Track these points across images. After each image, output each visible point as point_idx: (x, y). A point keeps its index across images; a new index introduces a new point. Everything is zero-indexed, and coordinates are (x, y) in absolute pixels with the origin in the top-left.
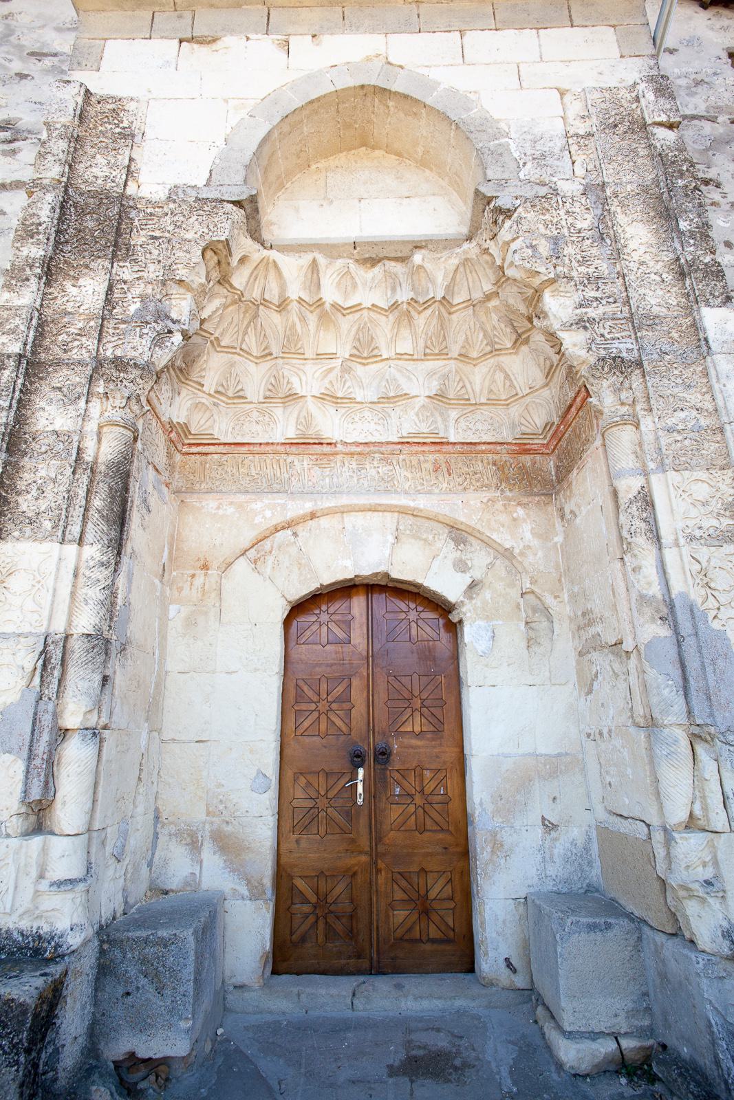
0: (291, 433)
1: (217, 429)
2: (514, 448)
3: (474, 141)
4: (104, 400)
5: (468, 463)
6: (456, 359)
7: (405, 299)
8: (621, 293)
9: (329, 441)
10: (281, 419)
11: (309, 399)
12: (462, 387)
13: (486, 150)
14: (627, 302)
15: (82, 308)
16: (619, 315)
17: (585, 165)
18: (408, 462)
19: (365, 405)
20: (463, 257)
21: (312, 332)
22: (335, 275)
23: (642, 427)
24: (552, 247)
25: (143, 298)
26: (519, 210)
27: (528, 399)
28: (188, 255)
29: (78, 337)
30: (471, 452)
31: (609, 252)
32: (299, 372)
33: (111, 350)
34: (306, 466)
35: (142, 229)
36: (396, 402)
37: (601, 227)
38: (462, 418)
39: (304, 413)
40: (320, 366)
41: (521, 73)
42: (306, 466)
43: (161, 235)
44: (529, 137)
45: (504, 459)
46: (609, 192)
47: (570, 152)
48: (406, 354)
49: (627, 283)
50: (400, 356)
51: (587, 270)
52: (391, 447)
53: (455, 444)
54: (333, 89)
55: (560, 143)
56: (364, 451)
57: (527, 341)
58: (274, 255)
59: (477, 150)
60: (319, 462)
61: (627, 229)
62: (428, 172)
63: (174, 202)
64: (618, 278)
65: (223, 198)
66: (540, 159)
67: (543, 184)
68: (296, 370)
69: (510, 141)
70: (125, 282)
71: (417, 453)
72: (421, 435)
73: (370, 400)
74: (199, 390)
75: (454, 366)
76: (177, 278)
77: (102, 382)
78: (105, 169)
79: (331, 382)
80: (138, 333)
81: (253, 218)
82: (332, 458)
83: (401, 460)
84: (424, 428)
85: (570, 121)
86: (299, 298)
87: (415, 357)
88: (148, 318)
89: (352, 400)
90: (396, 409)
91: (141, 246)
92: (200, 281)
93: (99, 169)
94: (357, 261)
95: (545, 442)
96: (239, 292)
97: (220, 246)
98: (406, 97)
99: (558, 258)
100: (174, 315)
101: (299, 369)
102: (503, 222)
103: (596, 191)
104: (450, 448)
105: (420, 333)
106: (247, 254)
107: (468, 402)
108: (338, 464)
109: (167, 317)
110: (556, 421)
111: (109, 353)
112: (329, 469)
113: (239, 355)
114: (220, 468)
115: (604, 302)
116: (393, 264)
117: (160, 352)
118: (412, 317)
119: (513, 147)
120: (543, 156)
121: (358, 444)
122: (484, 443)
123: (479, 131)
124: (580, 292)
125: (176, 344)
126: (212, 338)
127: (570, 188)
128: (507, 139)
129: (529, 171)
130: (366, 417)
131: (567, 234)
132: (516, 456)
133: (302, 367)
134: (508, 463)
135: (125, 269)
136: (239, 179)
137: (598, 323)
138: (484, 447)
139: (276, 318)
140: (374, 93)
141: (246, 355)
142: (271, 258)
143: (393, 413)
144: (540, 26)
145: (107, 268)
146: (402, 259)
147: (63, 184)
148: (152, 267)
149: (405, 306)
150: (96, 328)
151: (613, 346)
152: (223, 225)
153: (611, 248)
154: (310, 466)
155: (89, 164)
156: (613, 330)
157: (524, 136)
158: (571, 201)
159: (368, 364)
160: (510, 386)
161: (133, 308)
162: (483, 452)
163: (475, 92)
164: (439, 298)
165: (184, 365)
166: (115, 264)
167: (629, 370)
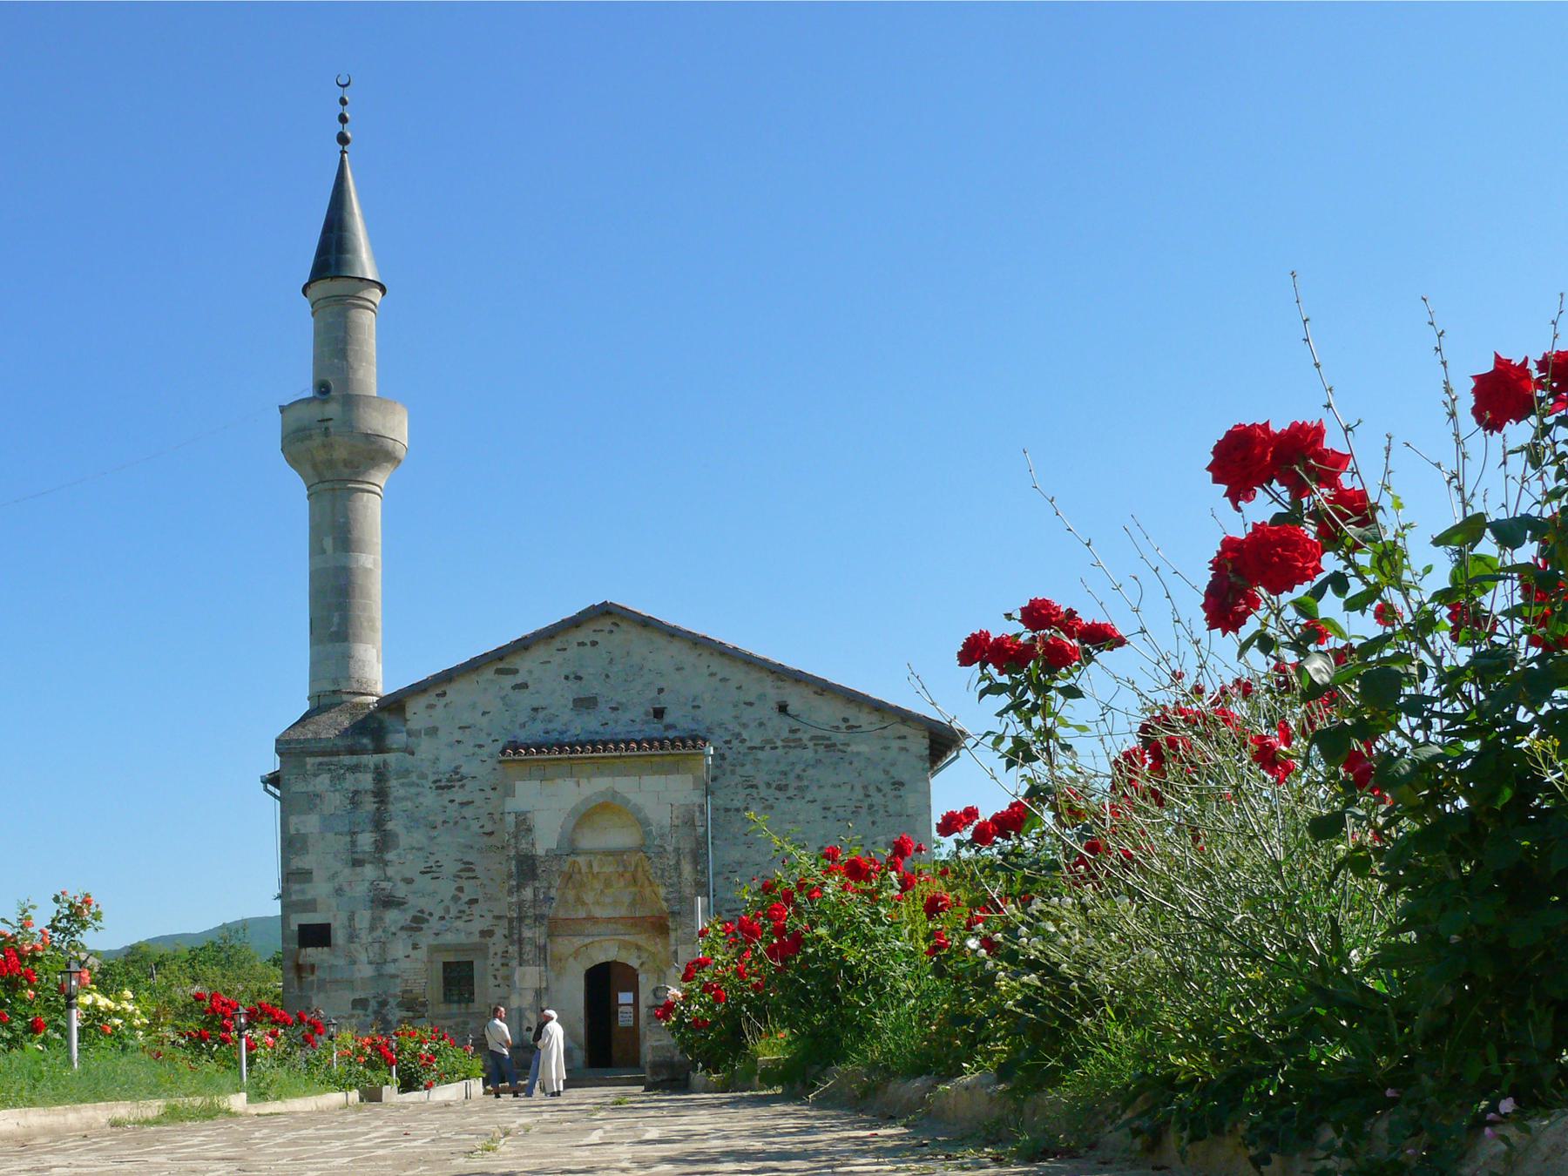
0: (584, 916)
56: (609, 920)
66: (662, 836)
103: (677, 850)
127: (670, 849)
144: (668, 772)
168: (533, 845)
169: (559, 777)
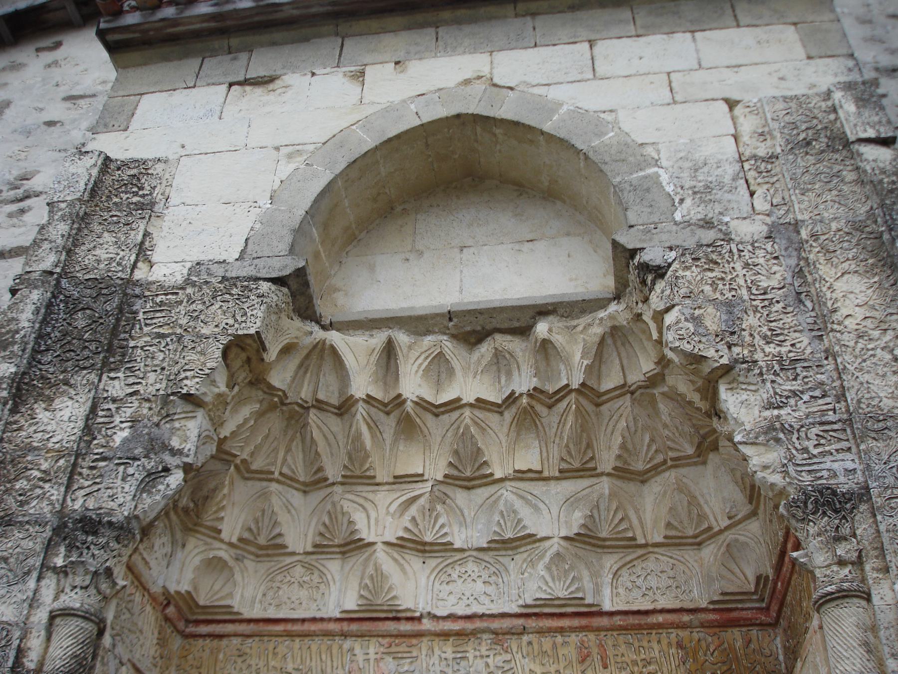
0: (351, 603)
1: (238, 597)
2: (712, 616)
3: (609, 174)
4: (62, 575)
5: (636, 644)
6: (609, 475)
7: (524, 389)
8: (833, 381)
9: (409, 614)
10: (337, 578)
11: (380, 547)
12: (622, 520)
13: (627, 186)
14: (841, 396)
15: (54, 440)
16: (831, 417)
17: (769, 198)
18: (536, 646)
19: (467, 554)
20: (609, 324)
21: (388, 442)
22: (420, 361)
23: (875, 599)
24: (724, 317)
25: (134, 421)
26: (675, 266)
27: (729, 536)
28: (202, 359)
29: (41, 483)
30: (640, 627)
31: (810, 320)
32: (368, 505)
33: (80, 502)
34: (372, 656)
35: (146, 325)
36: (516, 548)
37: (796, 284)
38: (625, 569)
39: (370, 570)
40: (399, 494)
41: (673, 85)
42: (372, 656)
43: (170, 331)
44: (687, 164)
45: (696, 636)
46: (804, 234)
47: (747, 181)
48: (530, 471)
49: (841, 367)
50: (521, 476)
51: (778, 349)
52: (506, 623)
53: (611, 614)
54: (417, 122)
55: (731, 169)
57: (715, 448)
58: (334, 337)
59: (614, 187)
60: (393, 649)
61: (837, 285)
62: (559, 203)
63: (193, 284)
64: (826, 358)
65: (259, 275)
66: (704, 193)
67: (707, 224)
68: (361, 501)
69: (661, 171)
70: (114, 400)
71: (550, 630)
72: (556, 602)
73: (476, 545)
74: (215, 538)
75: (606, 486)
76: (184, 391)
77: (62, 549)
78: (111, 249)
79: (413, 519)
80: (121, 474)
81: (302, 294)
82: (414, 641)
83: (524, 644)
84: (560, 591)
85: (745, 139)
86: (368, 395)
87: (546, 474)
88: (136, 452)
89: (447, 548)
90: (516, 557)
91: (142, 348)
92: (216, 390)
93: (104, 251)
94: (454, 337)
95: (764, 605)
96: (280, 393)
97: (249, 341)
98: (517, 124)
99: (733, 333)
100: (175, 443)
101: (366, 498)
102: (654, 283)
104: (605, 621)
105: (553, 435)
106: (295, 341)
107: (633, 543)
108: (424, 653)
109: (166, 447)
110: (770, 573)
111: (77, 505)
112: (409, 660)
113: (278, 481)
114: (240, 660)
115: (806, 397)
116: (509, 337)
117: (149, 501)
118: (537, 414)
119: (664, 177)
120: (708, 189)
121: (452, 617)
122: (662, 611)
123: (616, 161)
124: (768, 385)
125: (173, 486)
126: (238, 461)
128: (656, 169)
129: (688, 210)
130: (470, 572)
131: (746, 297)
132: (717, 630)
133: (370, 496)
134: (703, 644)
135: (116, 382)
136: (283, 247)
137: (798, 431)
138: (660, 618)
139: (334, 423)
140: (474, 121)
141: (289, 482)
142: (328, 342)
143: (512, 566)
145: (93, 383)
146: (524, 331)
147: (55, 276)
148: (152, 377)
149: (525, 400)
150: (66, 469)
151: (822, 466)
152: (254, 312)
153: (813, 314)
154: (378, 656)
155: (92, 245)
156: (823, 441)
157: (680, 163)
158: (750, 248)
159: (473, 487)
160: (699, 515)
161: (120, 436)
162: (660, 626)
163: (611, 111)
164: (575, 385)
165: (192, 505)
166: (104, 377)
167: (848, 506)
168: (143, 251)
169: (295, 69)
